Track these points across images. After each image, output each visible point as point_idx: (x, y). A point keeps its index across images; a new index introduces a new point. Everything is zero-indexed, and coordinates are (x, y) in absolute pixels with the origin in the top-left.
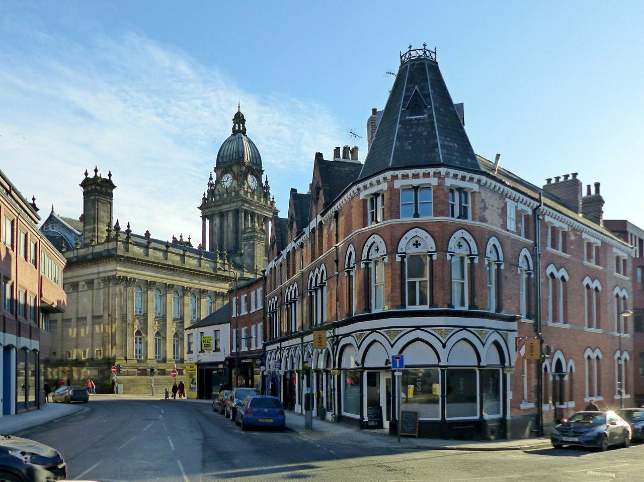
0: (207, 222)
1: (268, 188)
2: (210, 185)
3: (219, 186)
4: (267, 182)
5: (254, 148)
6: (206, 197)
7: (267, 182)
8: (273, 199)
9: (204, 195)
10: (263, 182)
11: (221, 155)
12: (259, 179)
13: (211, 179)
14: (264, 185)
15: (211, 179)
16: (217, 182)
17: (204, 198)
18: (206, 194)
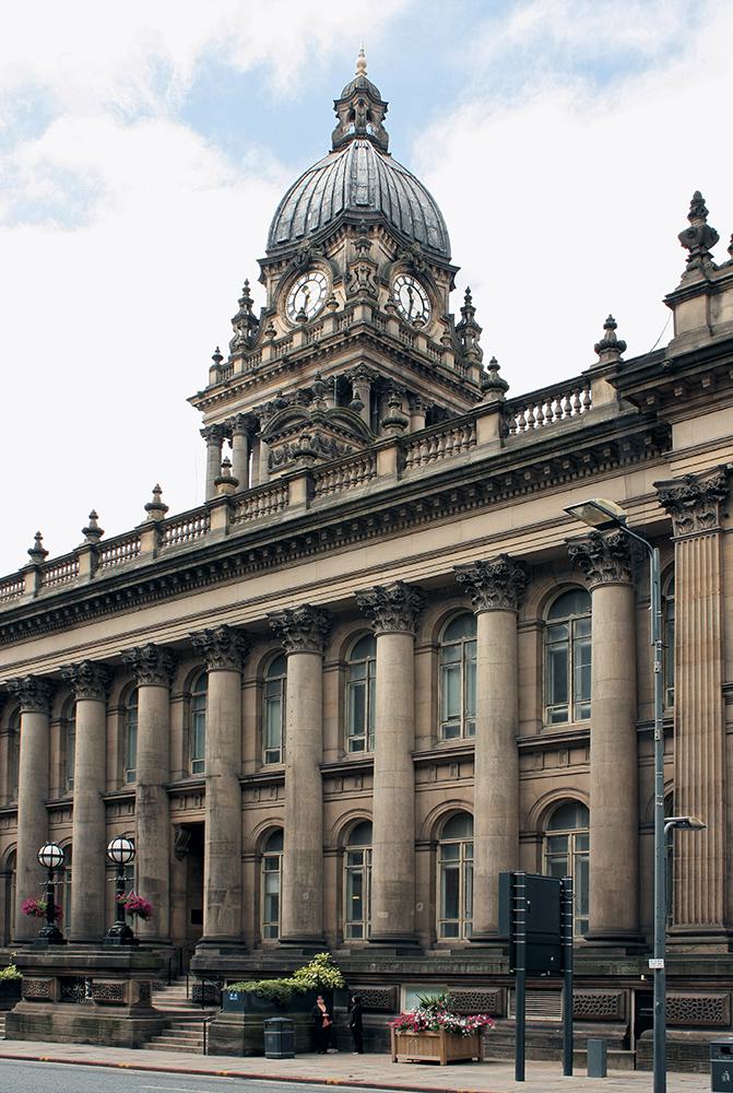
1: (469, 328)
2: (245, 320)
4: (468, 310)
5: (421, 196)
7: (468, 310)
9: (218, 358)
10: (455, 303)
11: (288, 213)
13: (247, 302)
14: (458, 319)
15: (247, 302)
16: (269, 313)
18: (226, 353)
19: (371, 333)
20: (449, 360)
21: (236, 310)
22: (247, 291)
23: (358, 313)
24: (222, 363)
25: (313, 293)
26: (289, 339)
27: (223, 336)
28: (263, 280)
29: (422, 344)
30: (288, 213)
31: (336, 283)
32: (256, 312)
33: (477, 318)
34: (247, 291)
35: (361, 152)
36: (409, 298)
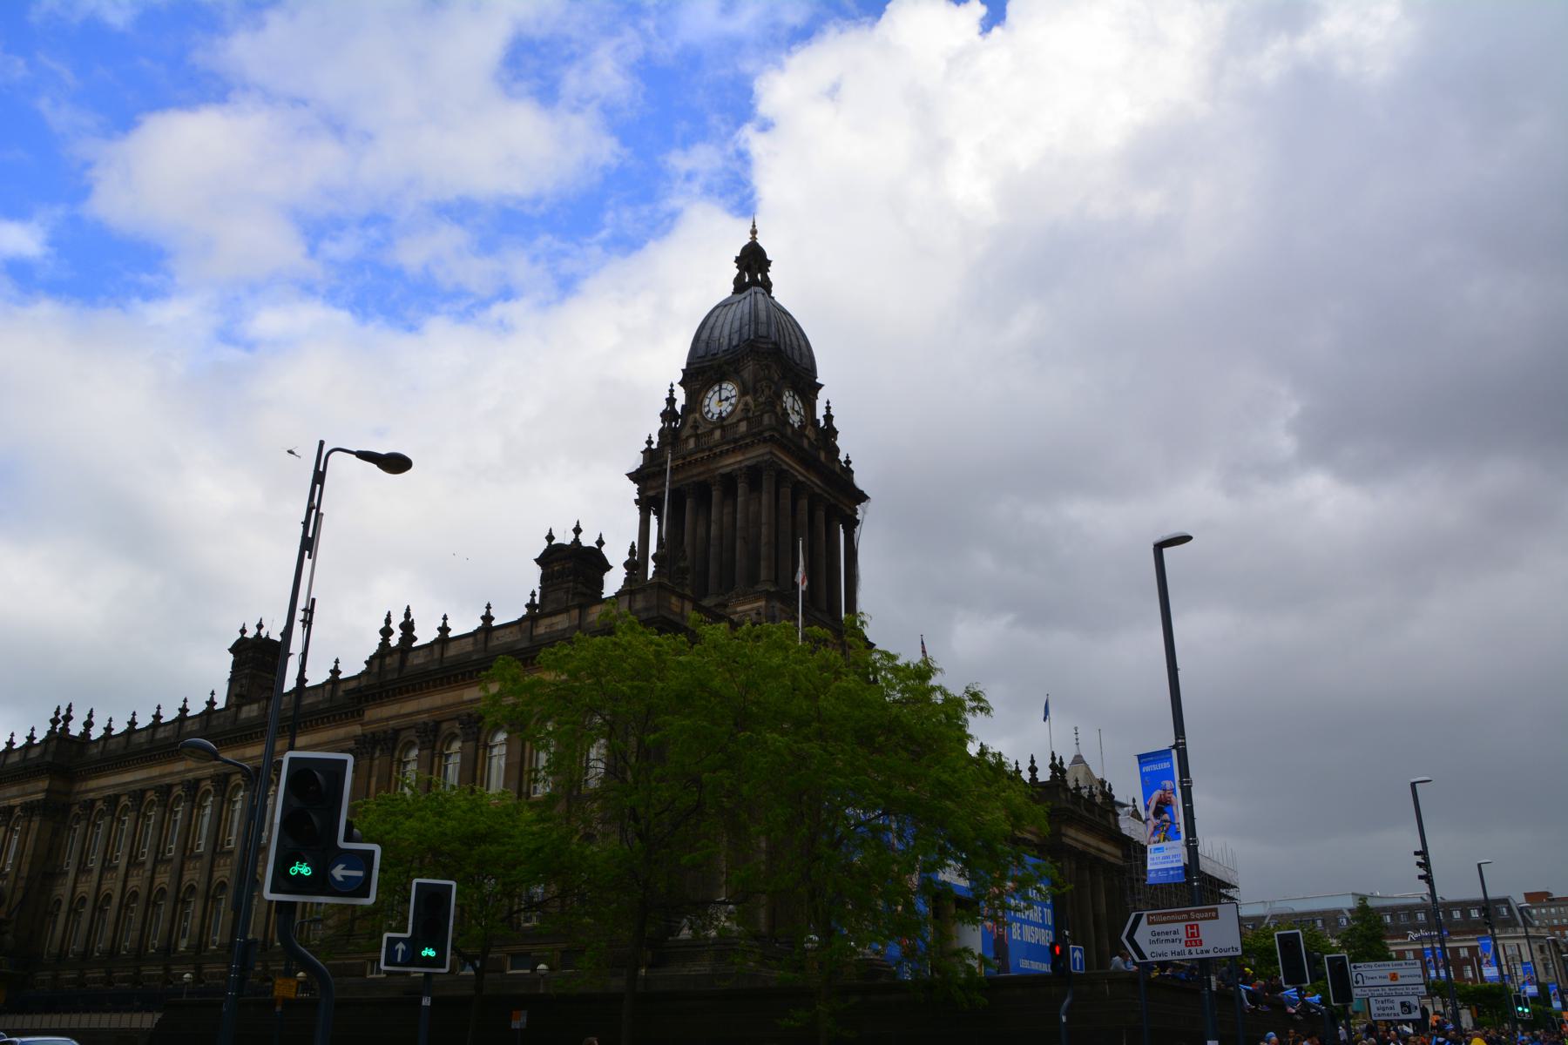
0: (653, 519)
1: (830, 432)
2: (668, 415)
3: (691, 418)
6: (654, 446)
8: (848, 462)
9: (650, 442)
10: (820, 413)
11: (705, 336)
12: (810, 406)
13: (671, 401)
14: (822, 423)
15: (671, 401)
17: (648, 453)
18: (656, 439)
20: (822, 456)
21: (663, 406)
22: (671, 391)
23: (766, 419)
24: (654, 446)
25: (721, 401)
26: (711, 432)
27: (654, 426)
28: (681, 383)
29: (805, 442)
30: (705, 336)
31: (743, 392)
32: (678, 407)
33: (835, 423)
34: (671, 391)
35: (760, 296)
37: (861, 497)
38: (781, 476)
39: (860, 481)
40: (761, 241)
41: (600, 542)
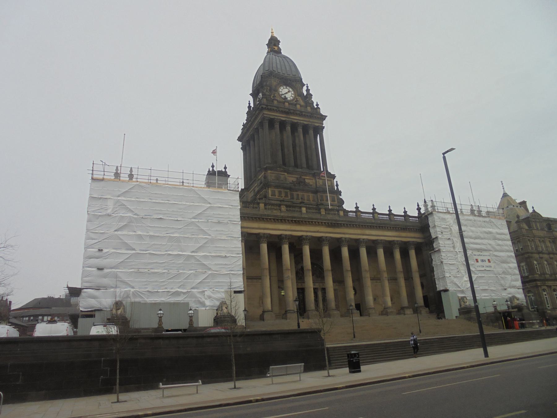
1: (309, 95)
4: (308, 90)
7: (308, 90)
8: (317, 105)
13: (249, 107)
19: (264, 106)
21: (247, 110)
22: (249, 104)
34: (249, 104)
36: (286, 92)
37: (323, 118)
38: (271, 122)
39: (323, 112)
40: (275, 35)
41: (225, 168)
